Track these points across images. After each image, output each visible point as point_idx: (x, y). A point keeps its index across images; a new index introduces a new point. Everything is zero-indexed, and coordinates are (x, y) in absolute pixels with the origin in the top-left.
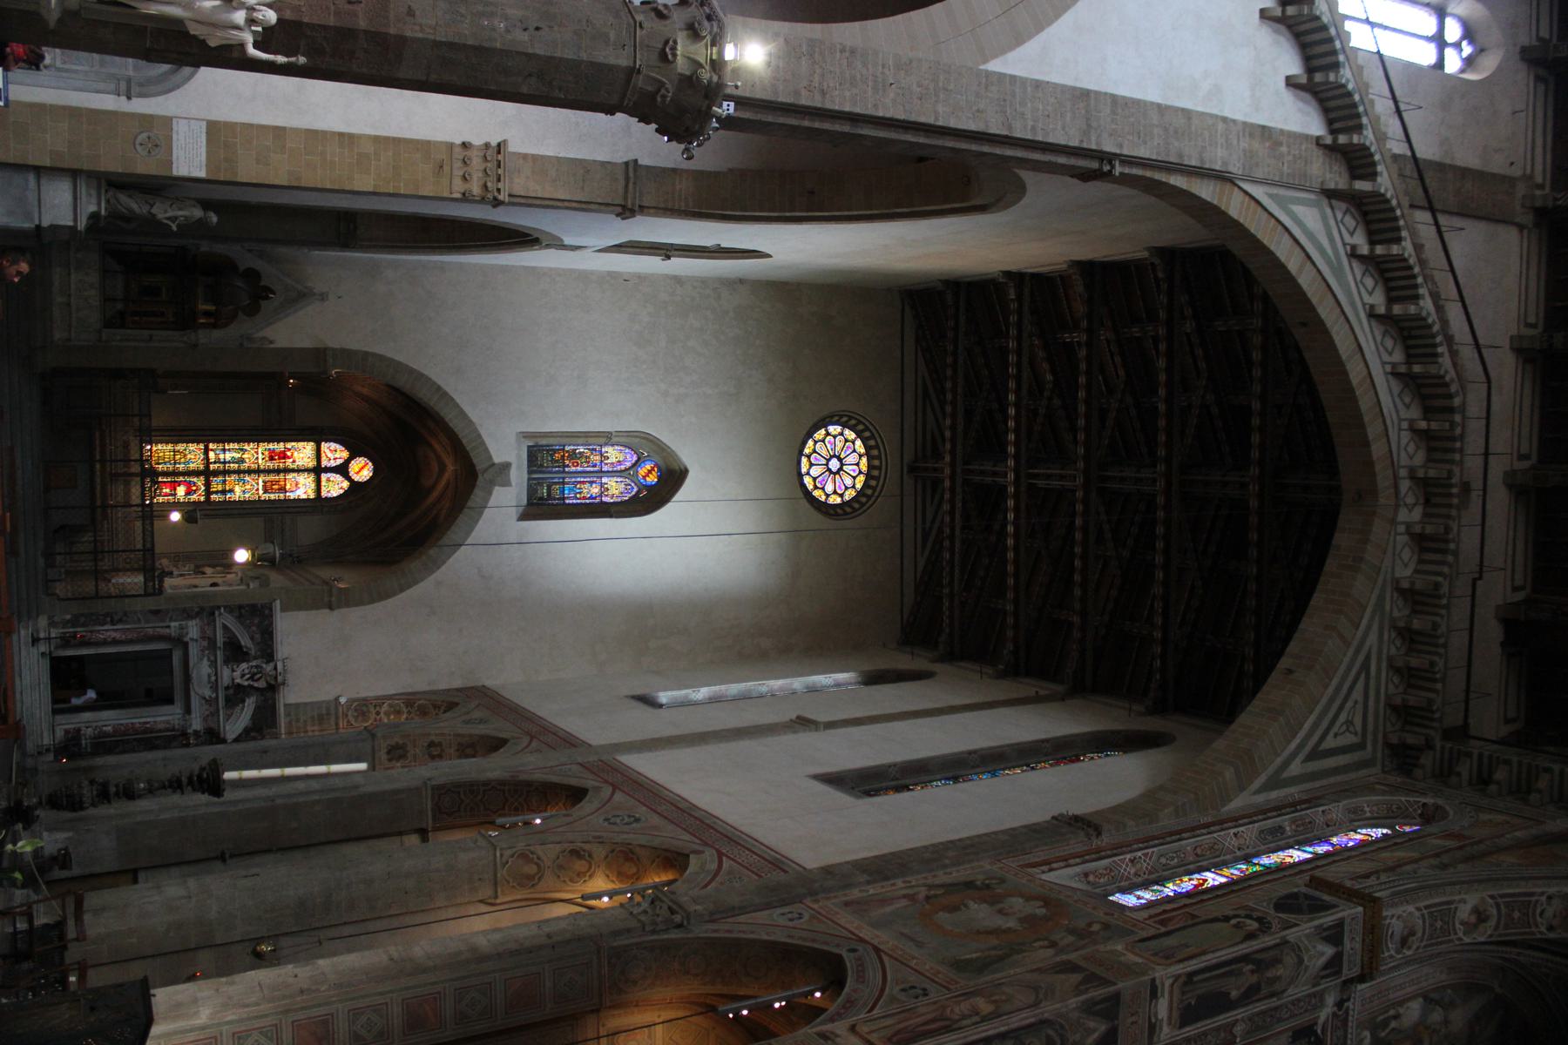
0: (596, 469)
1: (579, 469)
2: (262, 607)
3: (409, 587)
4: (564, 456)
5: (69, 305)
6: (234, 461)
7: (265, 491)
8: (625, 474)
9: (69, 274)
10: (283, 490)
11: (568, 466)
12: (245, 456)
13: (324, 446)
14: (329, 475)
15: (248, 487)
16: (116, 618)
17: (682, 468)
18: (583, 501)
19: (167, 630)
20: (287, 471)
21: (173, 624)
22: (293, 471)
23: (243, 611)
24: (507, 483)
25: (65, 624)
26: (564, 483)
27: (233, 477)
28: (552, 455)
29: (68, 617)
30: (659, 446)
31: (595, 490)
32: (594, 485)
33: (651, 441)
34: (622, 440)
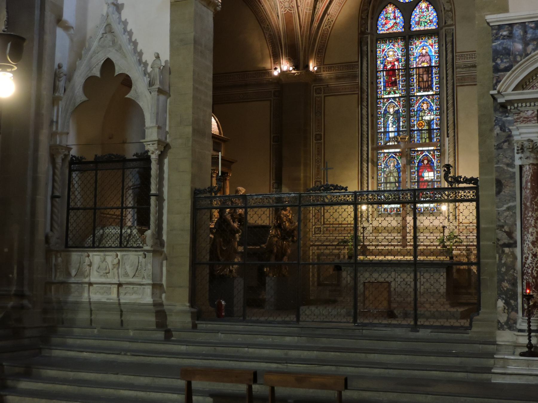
5: (120, 285)
6: (397, 121)
7: (430, 88)
9: (90, 284)
10: (428, 70)
12: (391, 110)
13: (382, 30)
14: (413, 22)
15: (425, 106)
16: (505, 240)
19: (526, 168)
20: (407, 67)
21: (518, 162)
22: (407, 60)
25: (510, 308)
27: (414, 122)
29: (501, 304)
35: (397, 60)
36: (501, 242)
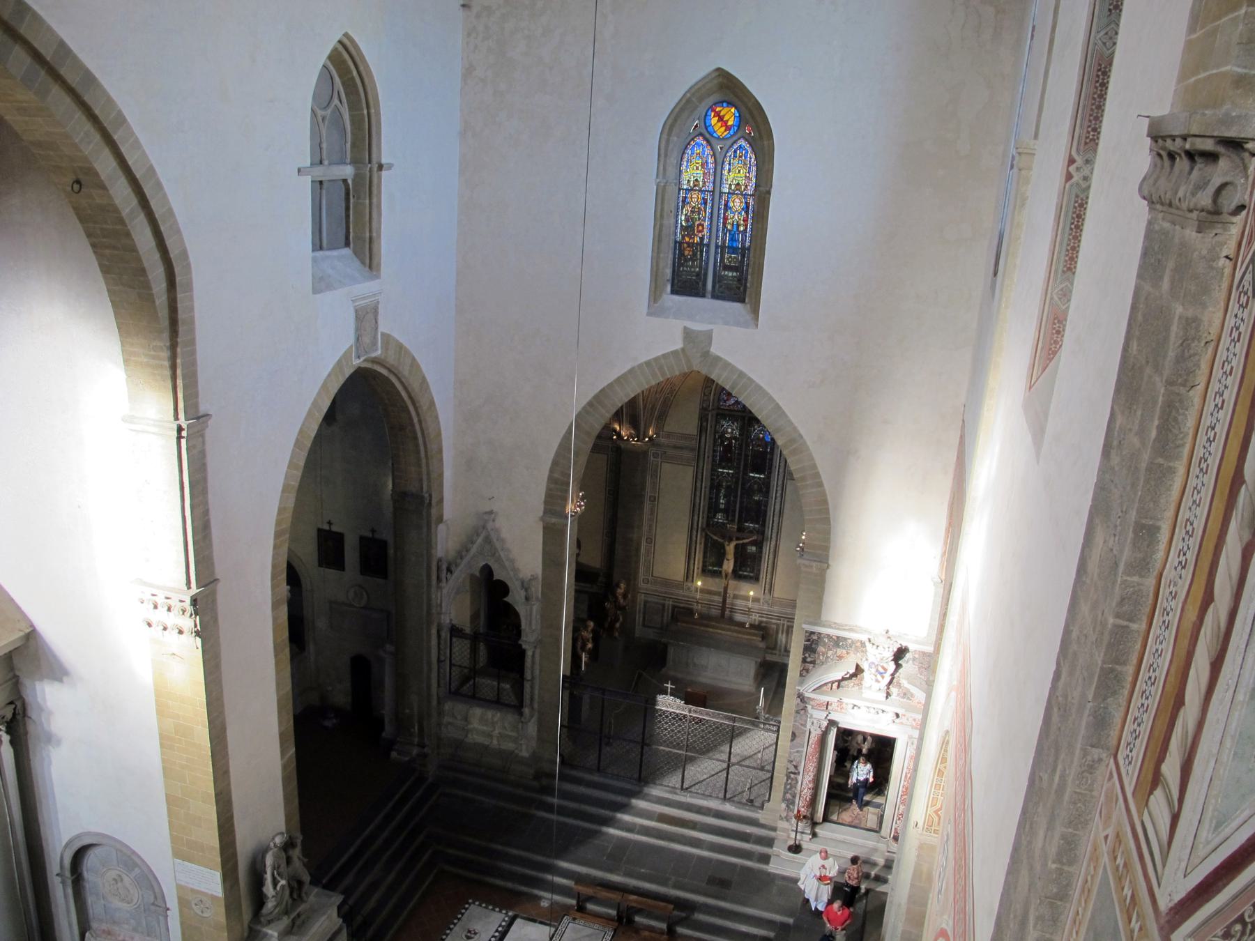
0: (709, 199)
1: (706, 224)
2: (808, 640)
3: (817, 475)
4: (687, 243)
8: (719, 161)
11: (702, 239)
12: (724, 484)
16: (792, 769)
17: (717, 74)
18: (750, 221)
23: (809, 660)
24: (709, 335)
26: (723, 247)
28: (686, 260)
30: (682, 110)
31: (737, 203)
32: (731, 204)
33: (675, 120)
34: (673, 160)
35: (735, 438)
36: (789, 771)
